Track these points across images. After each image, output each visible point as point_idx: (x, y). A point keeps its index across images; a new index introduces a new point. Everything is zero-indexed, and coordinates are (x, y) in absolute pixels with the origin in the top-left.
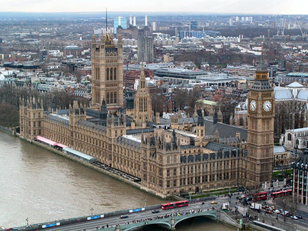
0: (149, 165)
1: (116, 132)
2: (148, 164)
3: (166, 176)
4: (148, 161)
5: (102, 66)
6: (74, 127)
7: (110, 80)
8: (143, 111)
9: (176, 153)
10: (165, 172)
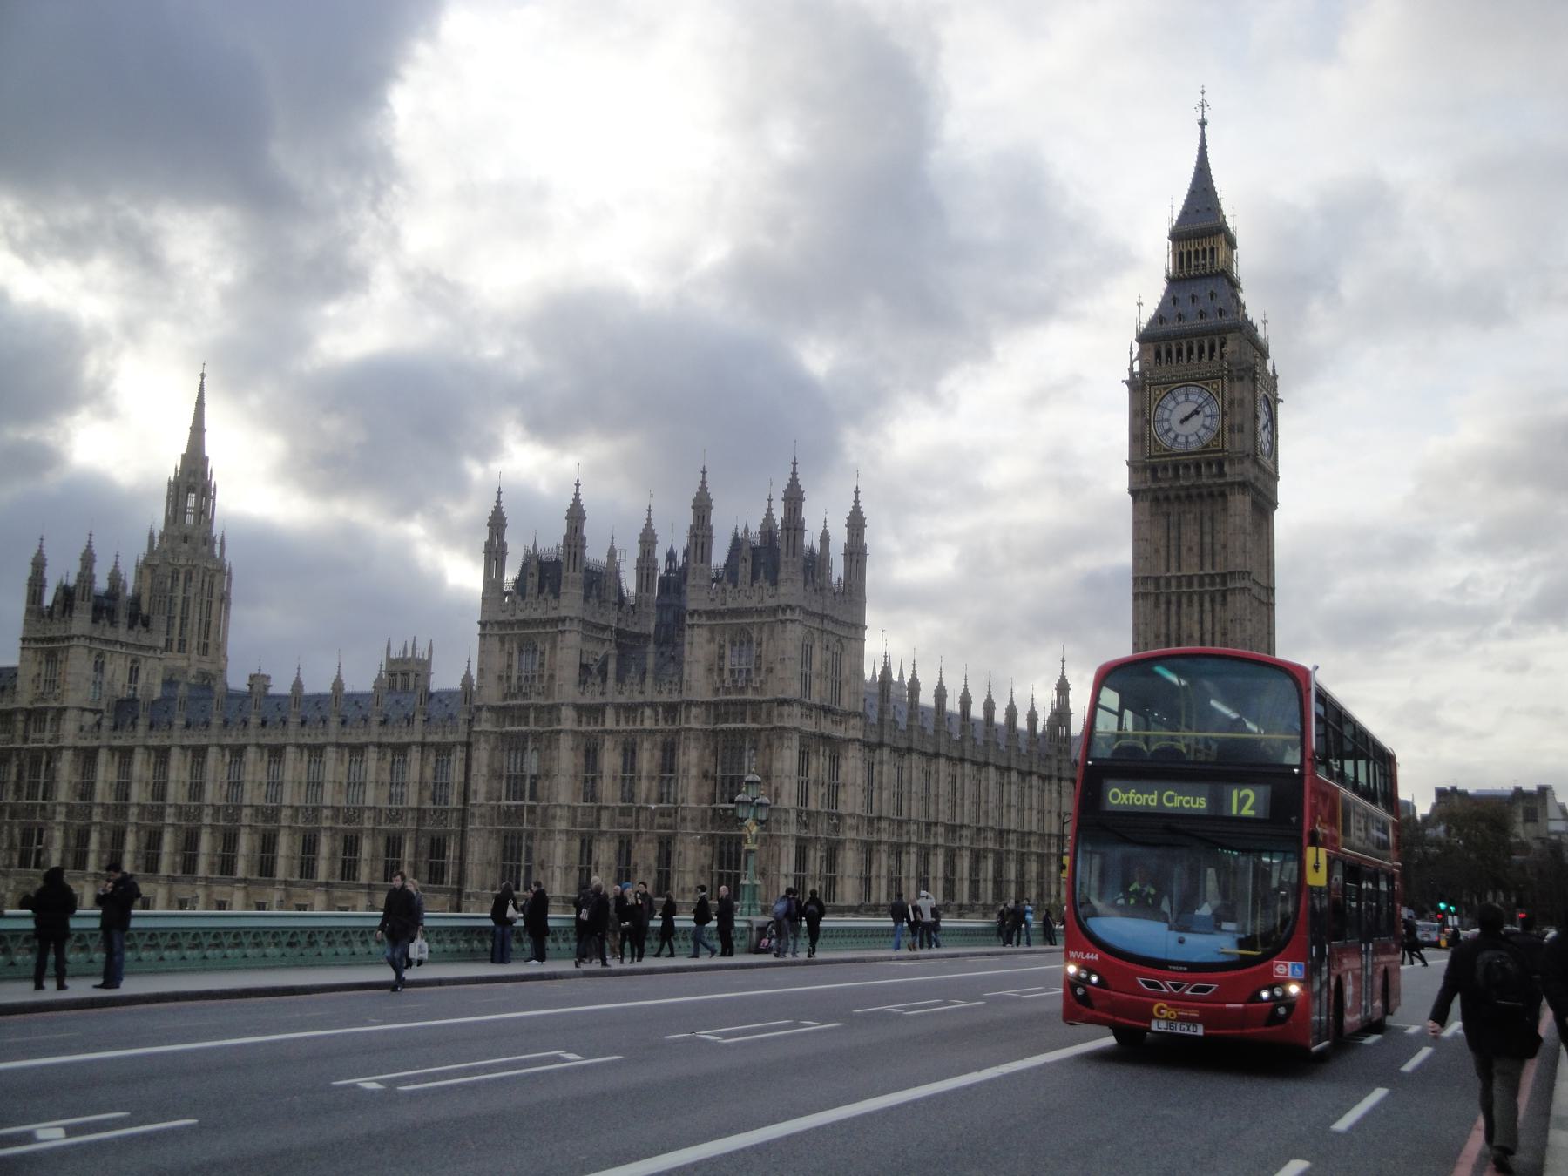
1: (99, 667)
2: (566, 743)
3: (794, 803)
8: (195, 643)
9: (844, 624)
10: (787, 759)
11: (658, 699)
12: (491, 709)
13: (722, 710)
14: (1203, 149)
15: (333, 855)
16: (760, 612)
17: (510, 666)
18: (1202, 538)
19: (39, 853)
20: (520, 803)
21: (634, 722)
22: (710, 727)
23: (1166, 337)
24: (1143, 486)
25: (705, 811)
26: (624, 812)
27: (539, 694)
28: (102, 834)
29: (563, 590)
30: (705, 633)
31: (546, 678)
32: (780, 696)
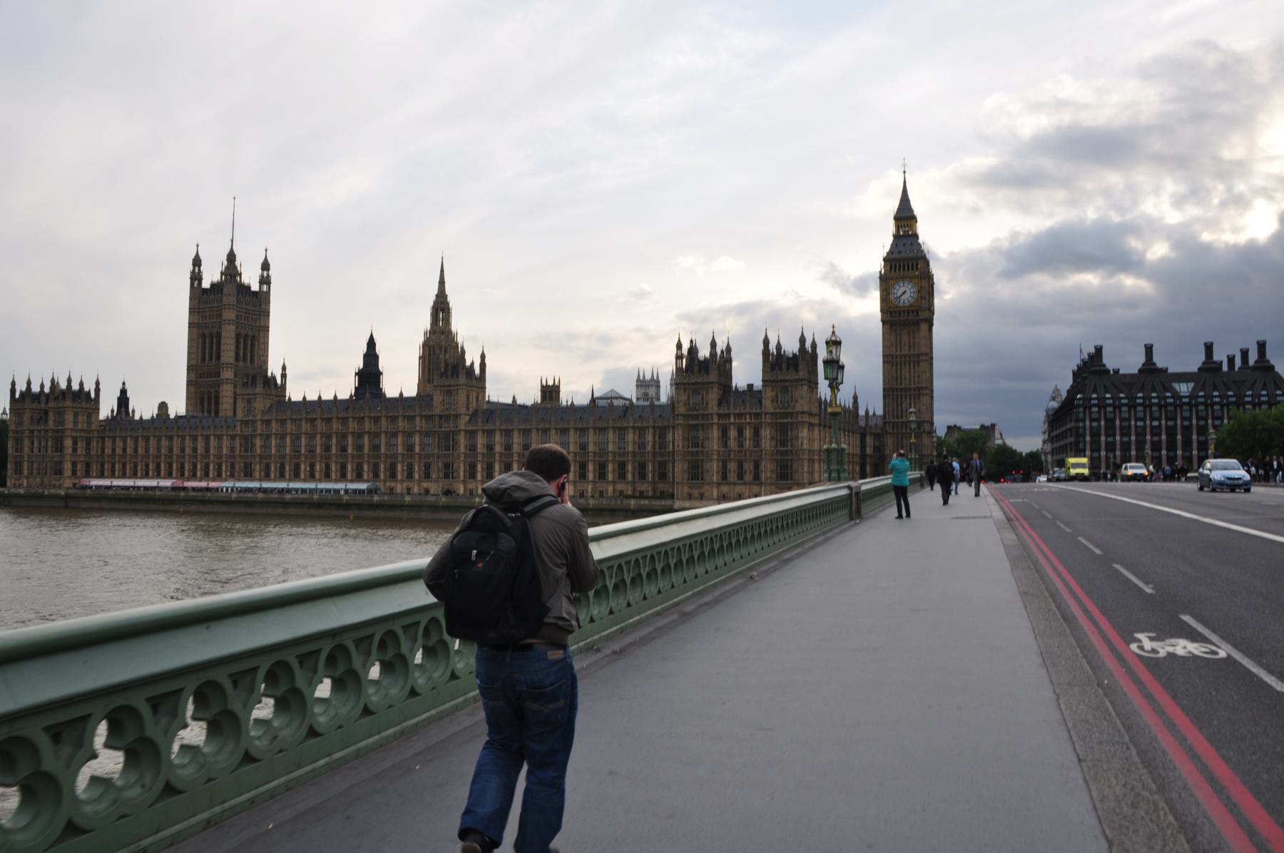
0: (718, 429)
1: (468, 398)
2: (715, 427)
4: (715, 417)
5: (229, 324)
6: (259, 423)
7: (241, 363)
11: (751, 411)
12: (682, 415)
13: (778, 416)
14: (905, 183)
15: (594, 470)
16: (791, 381)
17: (689, 399)
18: (910, 339)
19: (453, 473)
20: (697, 449)
21: (742, 419)
22: (774, 421)
23: (894, 260)
24: (887, 319)
25: (772, 451)
26: (741, 452)
27: (702, 410)
28: (482, 464)
29: (710, 372)
30: (770, 388)
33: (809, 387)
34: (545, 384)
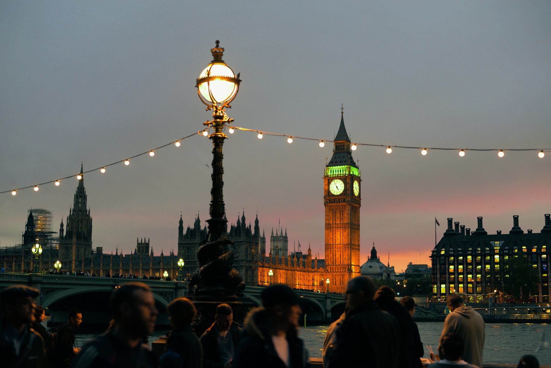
17: (185, 253)
27: (191, 259)
29: (196, 237)
31: (193, 255)
32: (241, 259)
33: (250, 246)
34: (140, 242)
